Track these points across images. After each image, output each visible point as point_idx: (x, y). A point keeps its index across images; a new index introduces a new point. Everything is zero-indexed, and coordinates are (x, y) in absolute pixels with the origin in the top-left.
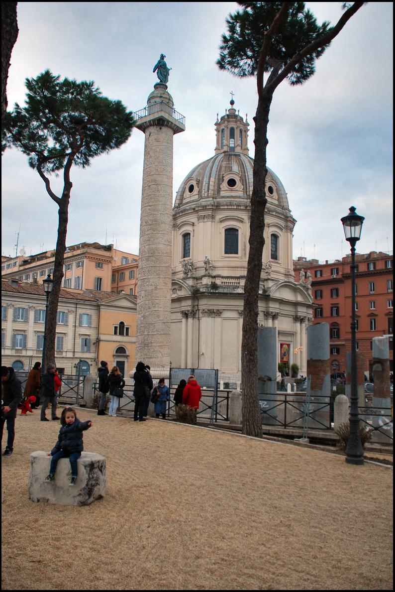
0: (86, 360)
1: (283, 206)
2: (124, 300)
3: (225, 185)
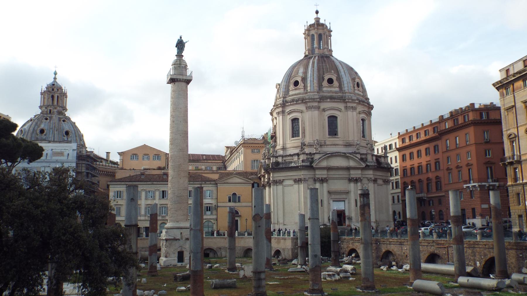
0: (210, 220)
1: (345, 90)
2: (235, 178)
3: (292, 87)
